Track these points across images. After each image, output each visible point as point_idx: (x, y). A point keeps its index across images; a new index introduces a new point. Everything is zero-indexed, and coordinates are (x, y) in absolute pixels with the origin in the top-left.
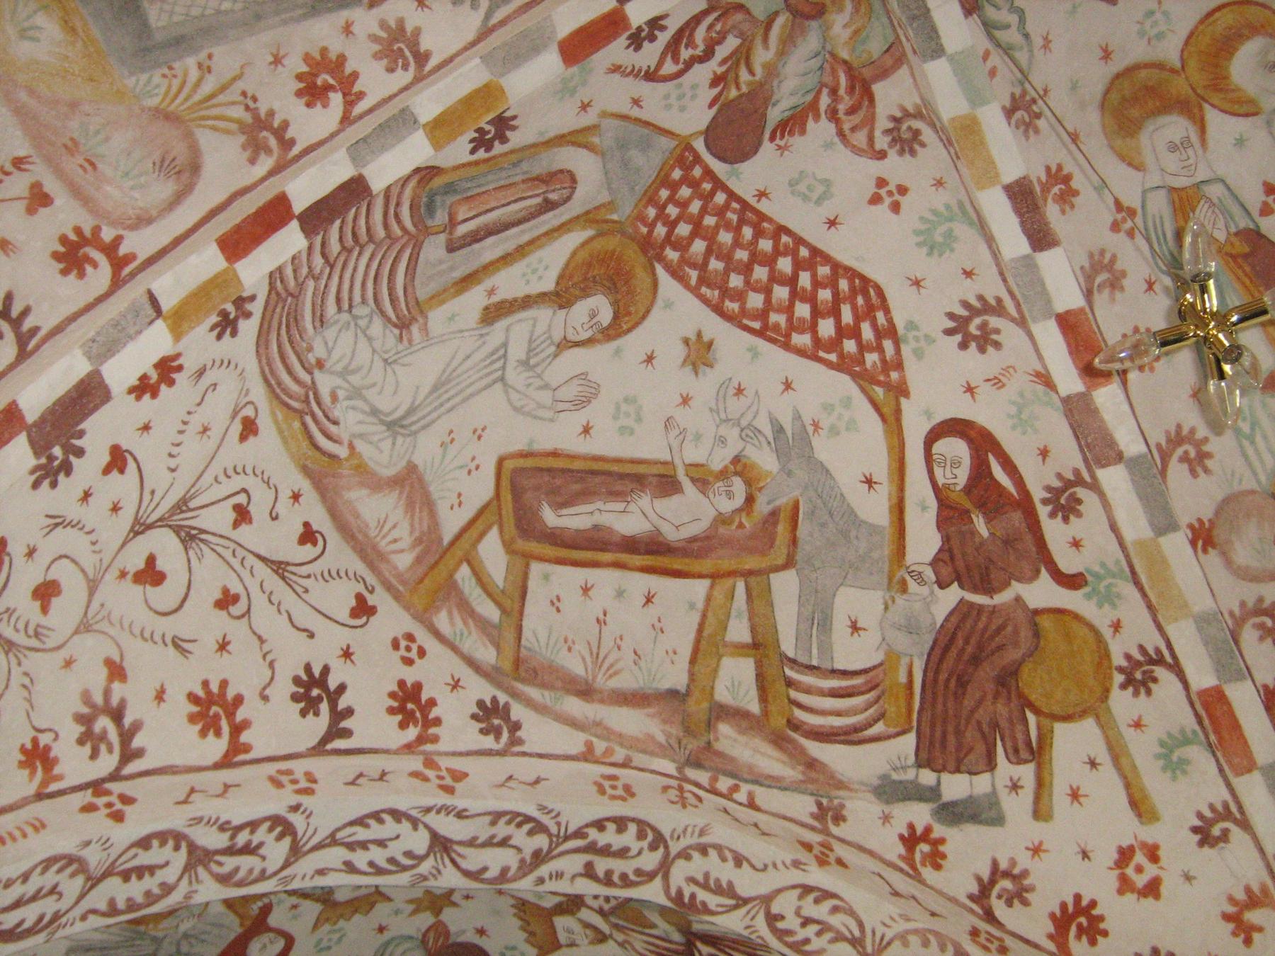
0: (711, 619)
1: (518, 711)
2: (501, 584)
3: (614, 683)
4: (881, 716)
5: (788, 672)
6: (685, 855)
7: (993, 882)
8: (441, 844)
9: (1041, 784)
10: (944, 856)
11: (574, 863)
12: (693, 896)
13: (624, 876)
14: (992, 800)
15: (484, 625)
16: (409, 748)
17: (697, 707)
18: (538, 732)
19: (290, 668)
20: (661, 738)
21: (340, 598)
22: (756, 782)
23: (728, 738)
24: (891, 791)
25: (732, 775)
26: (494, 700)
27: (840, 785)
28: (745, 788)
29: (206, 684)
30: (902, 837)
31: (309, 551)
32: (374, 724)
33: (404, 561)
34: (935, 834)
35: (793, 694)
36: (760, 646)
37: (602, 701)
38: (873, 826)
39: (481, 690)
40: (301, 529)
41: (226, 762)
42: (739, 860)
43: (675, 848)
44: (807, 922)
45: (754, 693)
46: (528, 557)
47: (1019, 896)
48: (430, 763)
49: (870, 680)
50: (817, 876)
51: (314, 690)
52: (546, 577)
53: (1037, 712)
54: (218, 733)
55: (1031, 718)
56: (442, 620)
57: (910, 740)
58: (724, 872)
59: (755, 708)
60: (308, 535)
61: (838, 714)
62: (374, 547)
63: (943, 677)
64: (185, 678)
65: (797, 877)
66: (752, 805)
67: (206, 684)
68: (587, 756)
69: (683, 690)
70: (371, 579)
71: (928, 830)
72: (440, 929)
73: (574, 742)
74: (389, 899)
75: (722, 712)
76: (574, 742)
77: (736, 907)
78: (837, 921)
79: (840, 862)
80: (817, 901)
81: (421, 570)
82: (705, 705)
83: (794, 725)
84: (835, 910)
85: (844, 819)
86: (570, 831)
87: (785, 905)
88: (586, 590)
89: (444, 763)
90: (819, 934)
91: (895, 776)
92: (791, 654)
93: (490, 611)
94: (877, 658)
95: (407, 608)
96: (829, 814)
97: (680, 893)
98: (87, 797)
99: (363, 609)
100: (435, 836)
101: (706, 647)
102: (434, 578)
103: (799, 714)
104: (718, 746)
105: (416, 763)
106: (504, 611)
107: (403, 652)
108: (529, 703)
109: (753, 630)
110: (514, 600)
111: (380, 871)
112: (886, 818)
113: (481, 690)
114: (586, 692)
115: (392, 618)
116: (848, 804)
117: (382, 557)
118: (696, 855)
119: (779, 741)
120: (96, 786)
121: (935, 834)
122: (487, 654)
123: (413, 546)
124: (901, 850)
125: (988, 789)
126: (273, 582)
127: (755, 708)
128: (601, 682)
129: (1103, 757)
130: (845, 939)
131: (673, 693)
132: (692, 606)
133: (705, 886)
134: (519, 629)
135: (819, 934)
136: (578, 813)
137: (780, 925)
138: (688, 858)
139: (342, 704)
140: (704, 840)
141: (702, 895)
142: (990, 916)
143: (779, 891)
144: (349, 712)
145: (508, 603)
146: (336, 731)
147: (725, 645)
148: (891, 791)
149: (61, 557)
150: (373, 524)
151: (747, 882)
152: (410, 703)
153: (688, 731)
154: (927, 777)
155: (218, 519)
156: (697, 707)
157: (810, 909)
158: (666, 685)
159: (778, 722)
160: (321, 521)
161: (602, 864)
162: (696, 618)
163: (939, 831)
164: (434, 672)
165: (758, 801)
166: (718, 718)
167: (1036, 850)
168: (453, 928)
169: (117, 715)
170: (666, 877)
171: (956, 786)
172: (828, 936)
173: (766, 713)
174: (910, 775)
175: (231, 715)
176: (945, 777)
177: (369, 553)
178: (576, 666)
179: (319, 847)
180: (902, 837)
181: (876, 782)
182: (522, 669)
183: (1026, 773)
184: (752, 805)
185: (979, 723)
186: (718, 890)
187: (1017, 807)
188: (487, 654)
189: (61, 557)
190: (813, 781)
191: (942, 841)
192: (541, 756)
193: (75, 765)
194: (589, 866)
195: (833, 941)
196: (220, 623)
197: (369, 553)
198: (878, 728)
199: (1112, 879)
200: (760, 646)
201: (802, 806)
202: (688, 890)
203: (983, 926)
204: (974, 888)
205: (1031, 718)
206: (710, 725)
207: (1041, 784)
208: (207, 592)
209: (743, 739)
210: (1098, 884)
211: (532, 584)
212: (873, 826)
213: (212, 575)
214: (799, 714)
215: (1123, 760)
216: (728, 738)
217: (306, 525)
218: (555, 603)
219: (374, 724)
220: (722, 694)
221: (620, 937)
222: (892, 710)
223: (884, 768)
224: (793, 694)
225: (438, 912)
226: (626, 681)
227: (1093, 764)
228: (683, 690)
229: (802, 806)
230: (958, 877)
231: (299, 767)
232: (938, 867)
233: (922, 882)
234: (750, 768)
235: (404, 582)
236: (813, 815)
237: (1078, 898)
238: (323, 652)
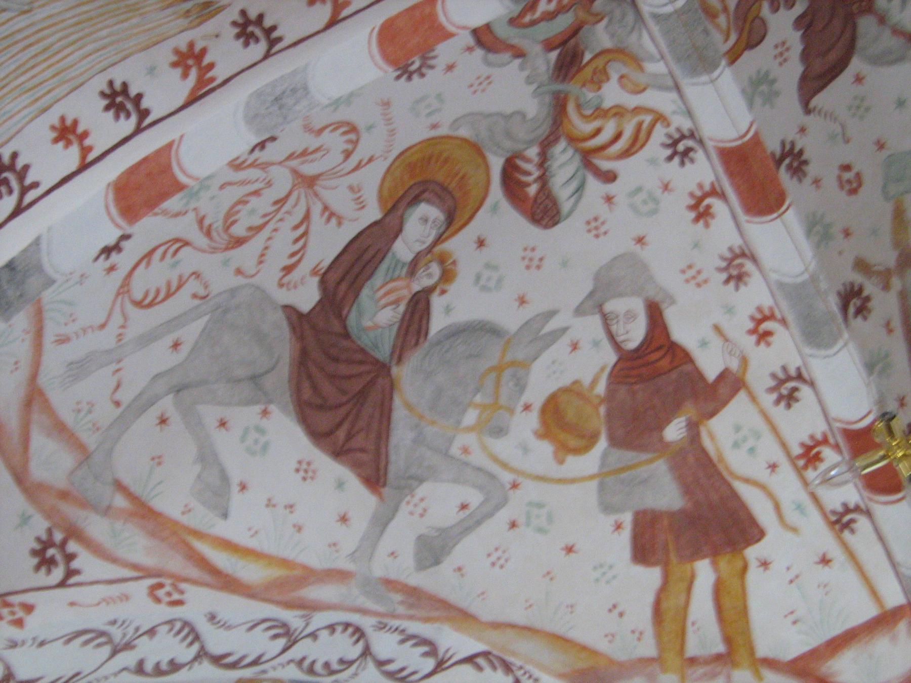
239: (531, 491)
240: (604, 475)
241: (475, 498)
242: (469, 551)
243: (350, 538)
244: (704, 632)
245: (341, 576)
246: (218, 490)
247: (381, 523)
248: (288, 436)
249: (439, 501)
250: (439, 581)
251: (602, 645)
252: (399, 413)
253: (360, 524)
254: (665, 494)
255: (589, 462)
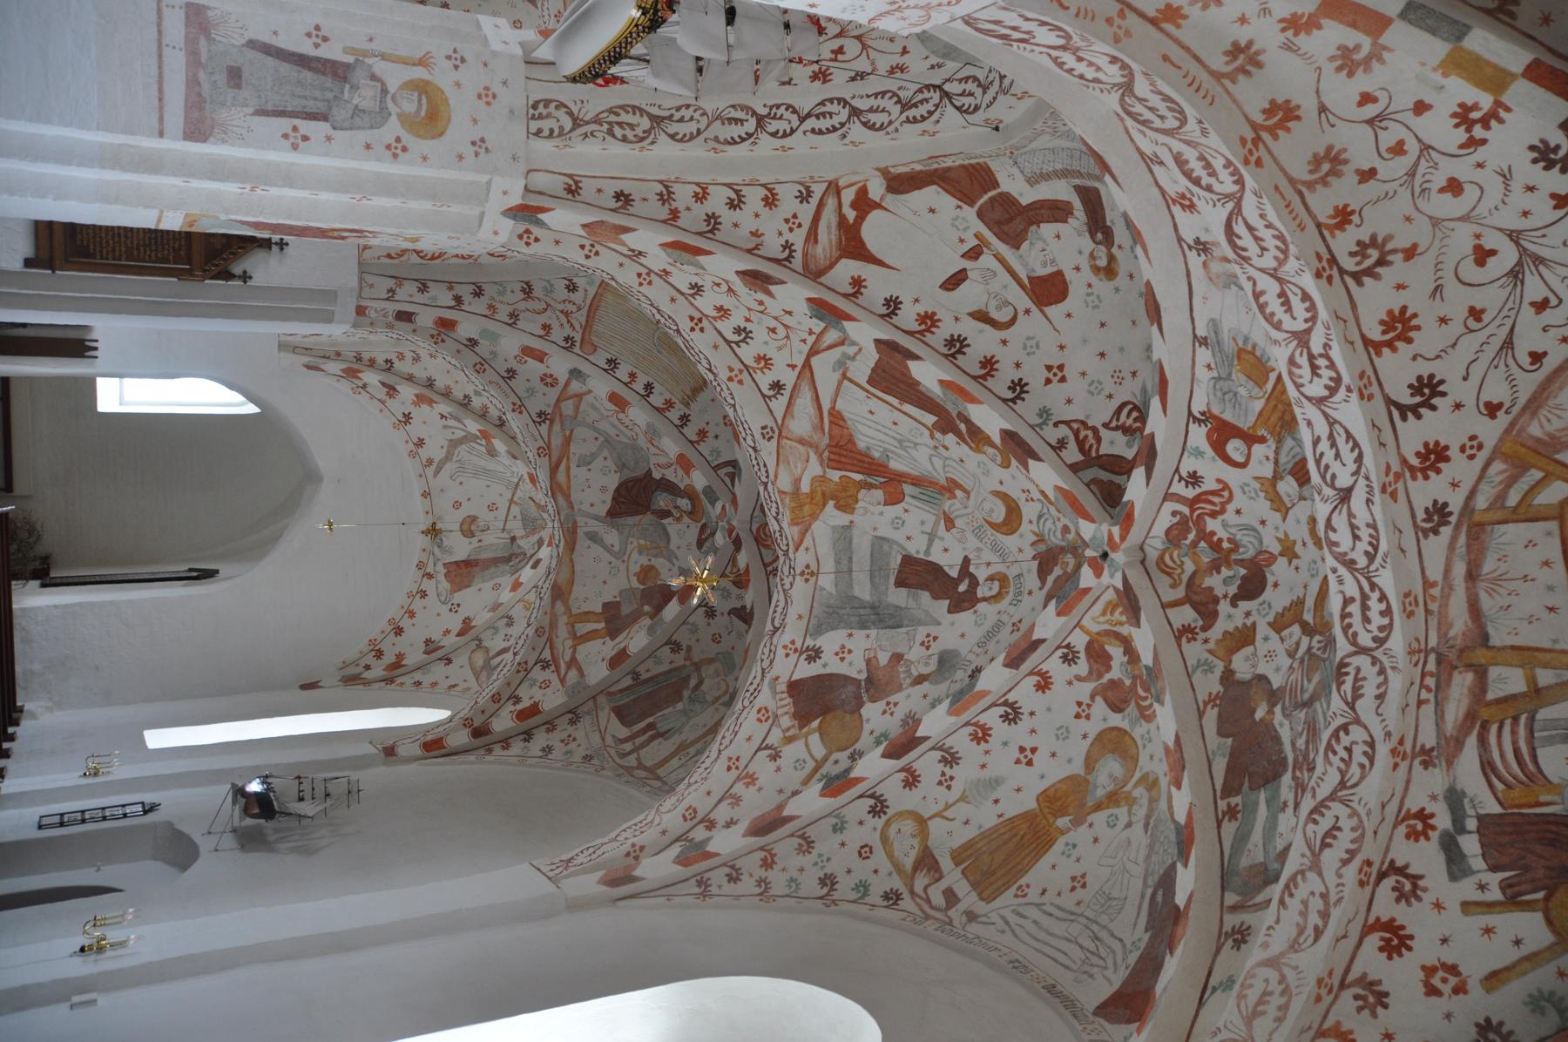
0: (1548, 656)
1: (1446, 531)
2: (1536, 502)
3: (1483, 596)
4: (1509, 786)
5: (1523, 718)
6: (1375, 661)
7: (1407, 876)
8: (1345, 495)
9: (1490, 907)
10: (1417, 840)
11: (1352, 589)
12: (1347, 674)
13: (1350, 626)
14: (1467, 872)
15: (1501, 497)
16: (1404, 461)
17: (1480, 656)
18: (1436, 546)
19: (1439, 369)
20: (1452, 633)
21: (1496, 391)
22: (1437, 703)
23: (1462, 681)
24: (1454, 799)
25: (1438, 686)
26: (1451, 514)
27: (1450, 764)
28: (1431, 696)
29: (1415, 315)
30: (1423, 809)
31: (1525, 360)
32: (1414, 435)
33: (1535, 430)
34: (1430, 833)
35: (1508, 722)
36: (1537, 695)
37: (1467, 588)
38: (1426, 788)
39: (1456, 502)
40: (1540, 351)
41: (1367, 342)
42: (1380, 697)
43: (1378, 654)
44: (1349, 750)
45: (1501, 694)
46: (1560, 518)
47: (1401, 896)
48: (1398, 476)
49: (1535, 777)
50: (1383, 750)
51: (1428, 390)
52: (1549, 534)
53: (1547, 899)
54: (1384, 332)
55: (1540, 895)
56: (1498, 466)
57: (1496, 809)
58: (1370, 690)
59: (1490, 696)
60: (1537, 357)
61: (1502, 756)
62: (1540, 407)
63: (1554, 828)
64: (1416, 300)
65: (1378, 734)
66: (1420, 703)
67: (1415, 315)
68: (1427, 584)
69: (1491, 643)
70: (1515, 410)
71: (1433, 828)
72: (1272, 559)
73: (1435, 573)
74: (1284, 519)
75: (1481, 673)
76: (1435, 573)
77: (1347, 703)
78: (1355, 771)
79: (1396, 766)
80: (1365, 753)
81: (1530, 443)
82: (1483, 661)
83: (1485, 726)
84: (1362, 766)
85: (1426, 768)
86: (1375, 580)
87: (1357, 733)
88: (1546, 563)
89: (1400, 485)
90: (1342, 760)
91: (1466, 801)
92: (1538, 716)
93: (1513, 499)
94: (1555, 779)
95: (1501, 440)
96: (1427, 758)
97: (1347, 665)
98: (1326, 256)
99: (1492, 410)
100: (1350, 490)
101: (1526, 655)
102: (1526, 454)
103: (1494, 728)
104: (1456, 673)
105: (1396, 467)
106: (1515, 508)
107: (1469, 444)
108: (1454, 539)
109: (1548, 688)
110: (1525, 514)
111: (1318, 462)
112: (1434, 797)
113: (1456, 502)
114: (1472, 576)
115: (1490, 431)
116: (1437, 771)
117: (1534, 414)
118: (1377, 668)
119: (1470, 716)
120: (1333, 261)
121: (1430, 833)
122: (1481, 502)
123: (1549, 435)
124: (1414, 810)
125: (1475, 868)
126: (1497, 343)
127: (1490, 696)
128: (1481, 587)
129: (1525, 950)
130: (1343, 777)
131: (1485, 637)
132: (1555, 641)
133: (1356, 680)
134: (1505, 522)
135: (1342, 760)
136: (1385, 579)
137: (1342, 734)
138: (1373, 664)
139: (1423, 411)
140: (1389, 671)
141: (1349, 680)
142: (1382, 876)
143: (1366, 728)
144: (1419, 417)
145: (1522, 510)
146: (1404, 410)
147: (1532, 669)
148: (1454, 799)
149: (1481, 188)
150: (1557, 401)
151: (1365, 706)
152: (1434, 456)
153: (1462, 651)
154: (1472, 824)
155: (1534, 289)
156: (1480, 656)
157: (1358, 750)
158: (1490, 630)
159: (1484, 714)
160: (1550, 364)
161: (1354, 608)
162: (1547, 645)
163: (1434, 835)
164: (1460, 469)
165: (1424, 707)
166: (1476, 672)
167: (1438, 906)
168: (1273, 567)
169: (1381, 262)
170: (1356, 653)
171: (1470, 845)
172: (1343, 766)
173: (1489, 704)
174: (1471, 812)
175: (1398, 338)
176: (1475, 837)
177: (1534, 404)
178: (1489, 565)
179: (1326, 415)
180: (1423, 809)
181: (1459, 788)
182: (1476, 530)
183: (1495, 894)
184: (1420, 703)
185: (1524, 858)
186: (1355, 689)
187: (1466, 889)
188: (1481, 502)
189: (1481, 188)
190: (1448, 743)
191: (1428, 838)
192: (1420, 552)
193: (1343, 243)
194: (1352, 600)
195: (1339, 769)
196: (1459, 313)
197: (1534, 404)
198: (1500, 786)
199: (1431, 961)
200: (1537, 695)
201: (1428, 738)
202: (1350, 669)
203: (1375, 870)
204: (1399, 863)
205: (1540, 895)
206: (1469, 666)
207: (1490, 907)
208: (1478, 299)
209: (1465, 691)
210: (1425, 951)
211: (1541, 524)
212: (1426, 788)
213: (1491, 299)
214: (1494, 728)
215: (1527, 965)
216: (1462, 681)
217: (1545, 354)
218: (1530, 544)
219: (1414, 435)
220: (1494, 672)
221: (1296, 665)
222: (1516, 793)
223: (1470, 792)
224: (1508, 722)
225: (1282, 554)
226: (1486, 602)
227: (1517, 942)
228: (1491, 643)
229: (1428, 738)
230: (1406, 852)
231: (1375, 389)
232: (1408, 836)
233: (1395, 827)
234: (1446, 699)
235: (1519, 431)
236: (1423, 746)
237: (1411, 937)
238: (1457, 389)
239: (623, 567)
240: (632, 590)
241: (616, 548)
242: (597, 550)
243: (586, 507)
244: (583, 628)
245: (572, 507)
246: (585, 462)
247: (596, 518)
248: (613, 481)
249: (612, 537)
250: (582, 542)
251: (573, 596)
252: (637, 518)
253: (593, 511)
254: (625, 610)
255: (635, 584)
